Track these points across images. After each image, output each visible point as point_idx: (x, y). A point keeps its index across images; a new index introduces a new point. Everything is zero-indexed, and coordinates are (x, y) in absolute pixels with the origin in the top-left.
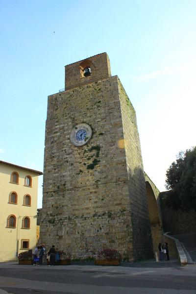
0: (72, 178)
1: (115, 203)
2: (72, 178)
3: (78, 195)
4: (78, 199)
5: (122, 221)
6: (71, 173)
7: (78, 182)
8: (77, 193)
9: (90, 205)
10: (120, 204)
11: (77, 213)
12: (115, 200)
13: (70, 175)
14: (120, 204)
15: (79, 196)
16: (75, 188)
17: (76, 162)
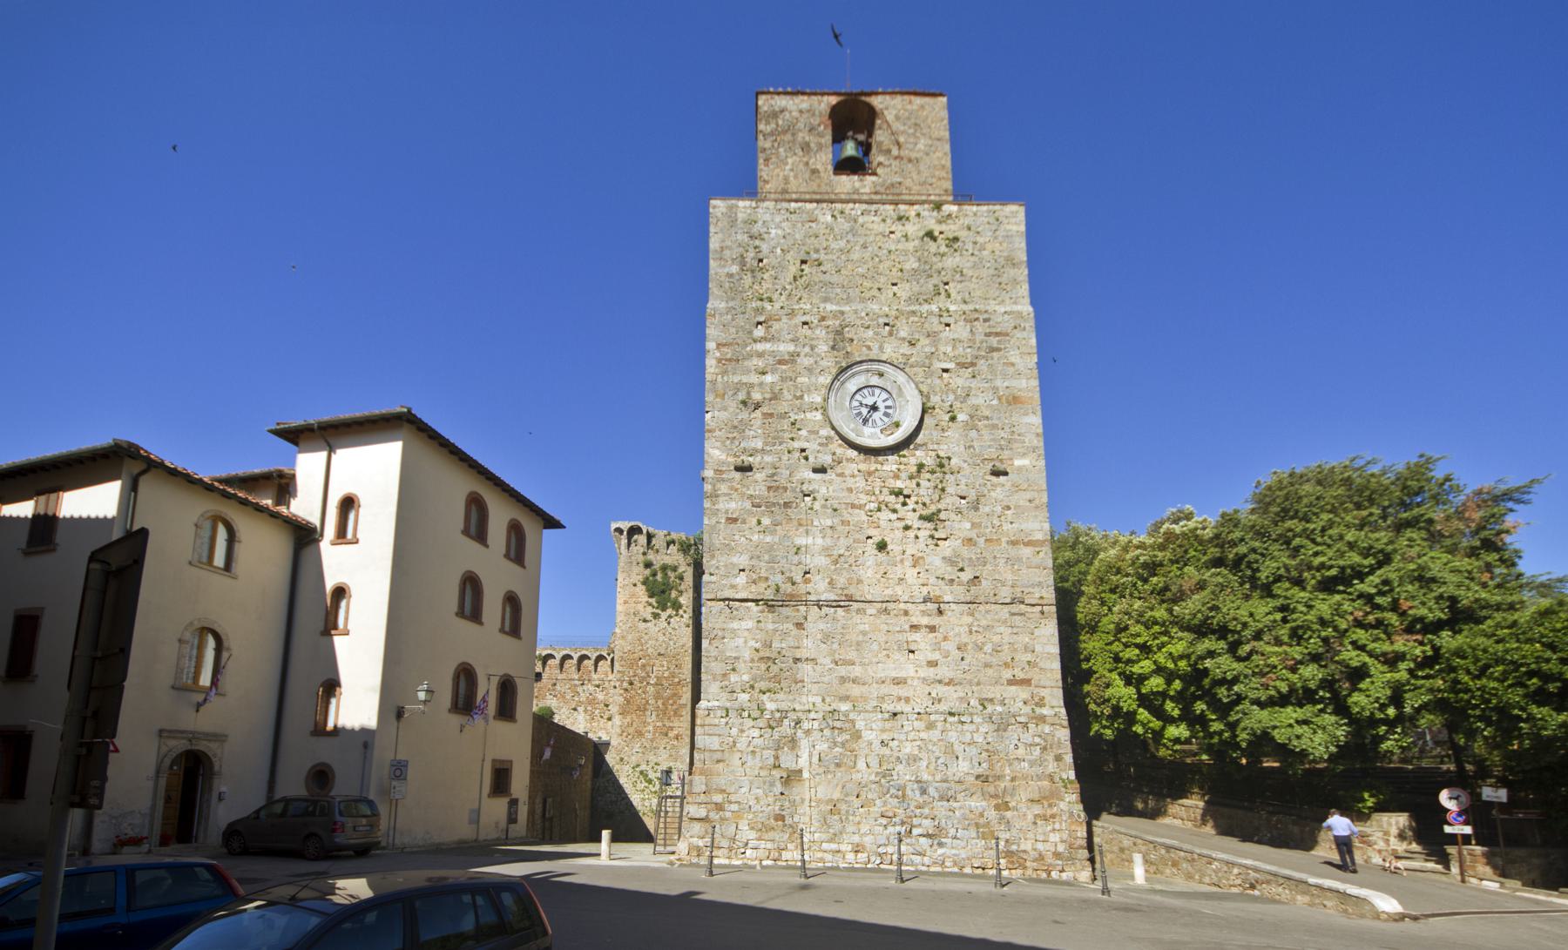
0: (836, 562)
1: (1007, 674)
2: (836, 562)
3: (861, 627)
4: (858, 644)
5: (1037, 740)
6: (829, 541)
7: (860, 582)
8: (857, 619)
9: (908, 671)
10: (1026, 682)
11: (855, 691)
12: (1006, 665)
13: (826, 551)
14: (1026, 682)
15: (864, 633)
16: (846, 602)
17: (853, 506)
